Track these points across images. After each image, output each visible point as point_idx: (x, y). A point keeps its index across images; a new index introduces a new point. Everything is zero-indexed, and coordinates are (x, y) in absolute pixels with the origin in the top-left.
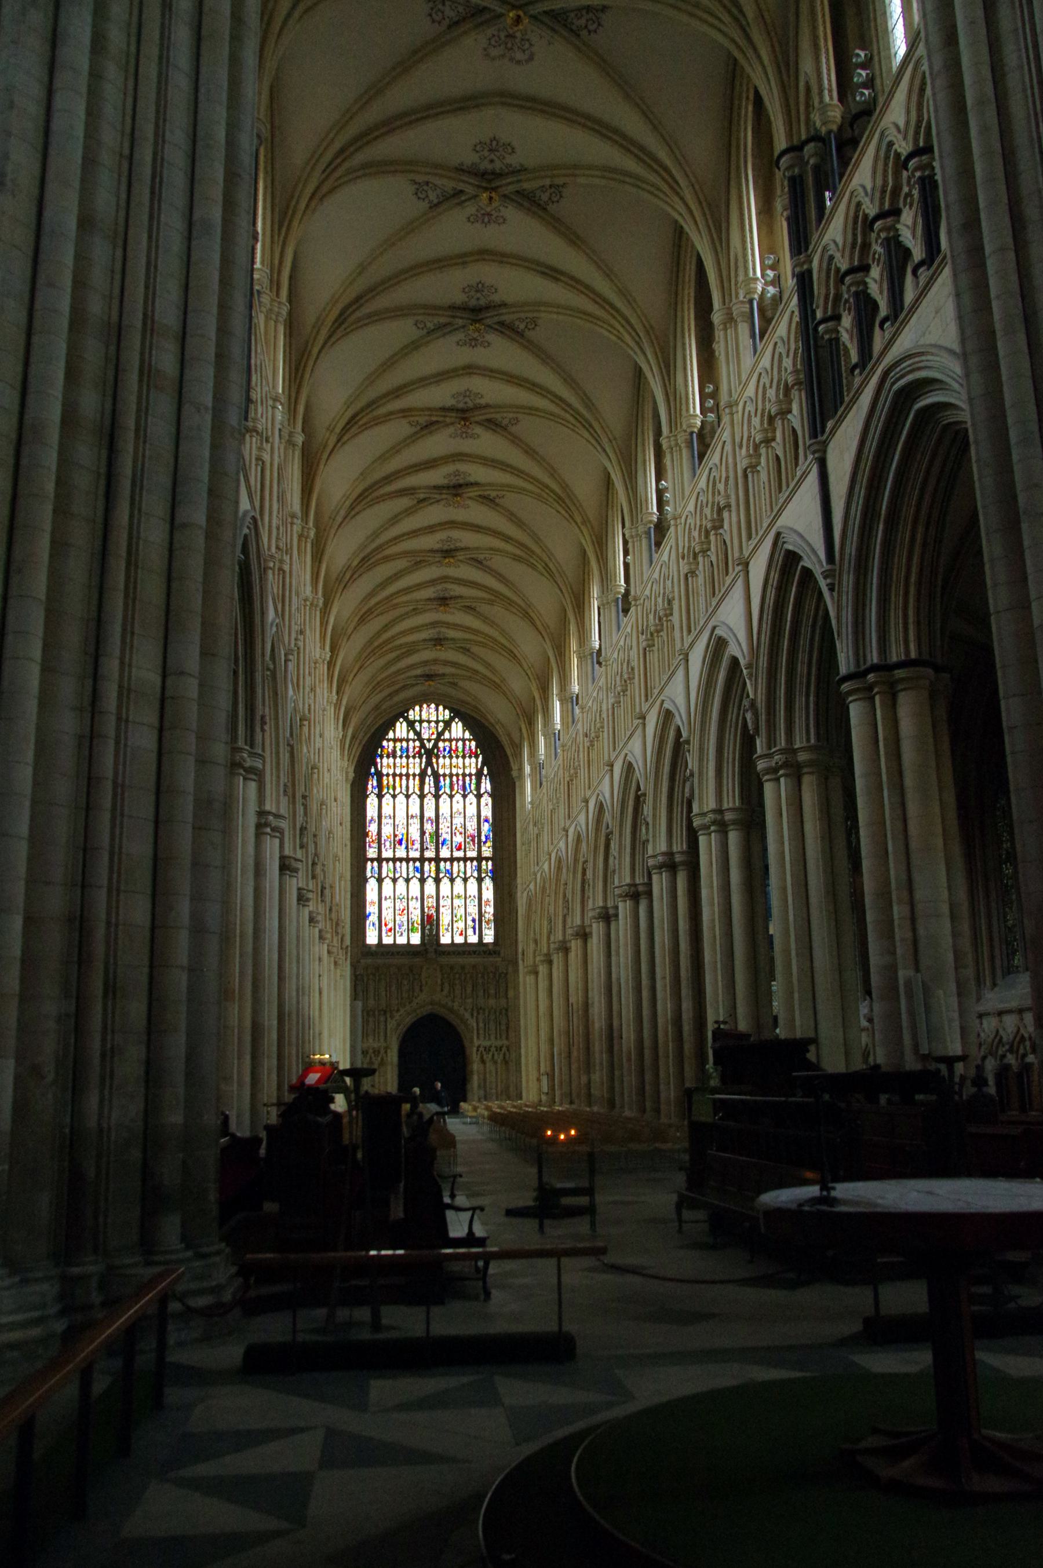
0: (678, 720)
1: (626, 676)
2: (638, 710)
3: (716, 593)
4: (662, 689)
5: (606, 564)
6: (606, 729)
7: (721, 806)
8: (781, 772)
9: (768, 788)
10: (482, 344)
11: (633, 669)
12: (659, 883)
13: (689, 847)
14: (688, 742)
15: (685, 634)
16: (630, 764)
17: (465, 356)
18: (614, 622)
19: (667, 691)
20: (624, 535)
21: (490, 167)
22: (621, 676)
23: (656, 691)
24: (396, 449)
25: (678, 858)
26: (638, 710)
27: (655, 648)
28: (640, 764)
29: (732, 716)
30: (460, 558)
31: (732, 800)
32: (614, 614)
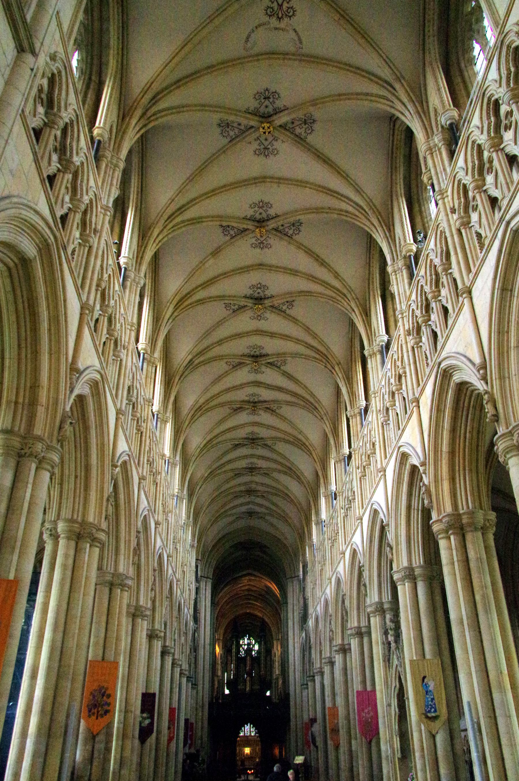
0: (381, 515)
1: (350, 498)
2: (358, 514)
3: (400, 429)
4: (371, 498)
5: (338, 440)
6: (340, 534)
7: (411, 564)
8: (450, 532)
9: (442, 544)
10: (264, 319)
11: (354, 492)
12: (375, 621)
13: (392, 598)
14: (388, 525)
15: (383, 458)
16: (355, 550)
17: (254, 325)
18: (343, 470)
19: (374, 499)
20: (347, 415)
21: (261, 217)
22: (348, 498)
23: (367, 501)
24: (219, 379)
26: (358, 514)
27: (367, 478)
28: (361, 549)
29: (415, 492)
30: (259, 443)
31: (418, 560)
32: (343, 466)
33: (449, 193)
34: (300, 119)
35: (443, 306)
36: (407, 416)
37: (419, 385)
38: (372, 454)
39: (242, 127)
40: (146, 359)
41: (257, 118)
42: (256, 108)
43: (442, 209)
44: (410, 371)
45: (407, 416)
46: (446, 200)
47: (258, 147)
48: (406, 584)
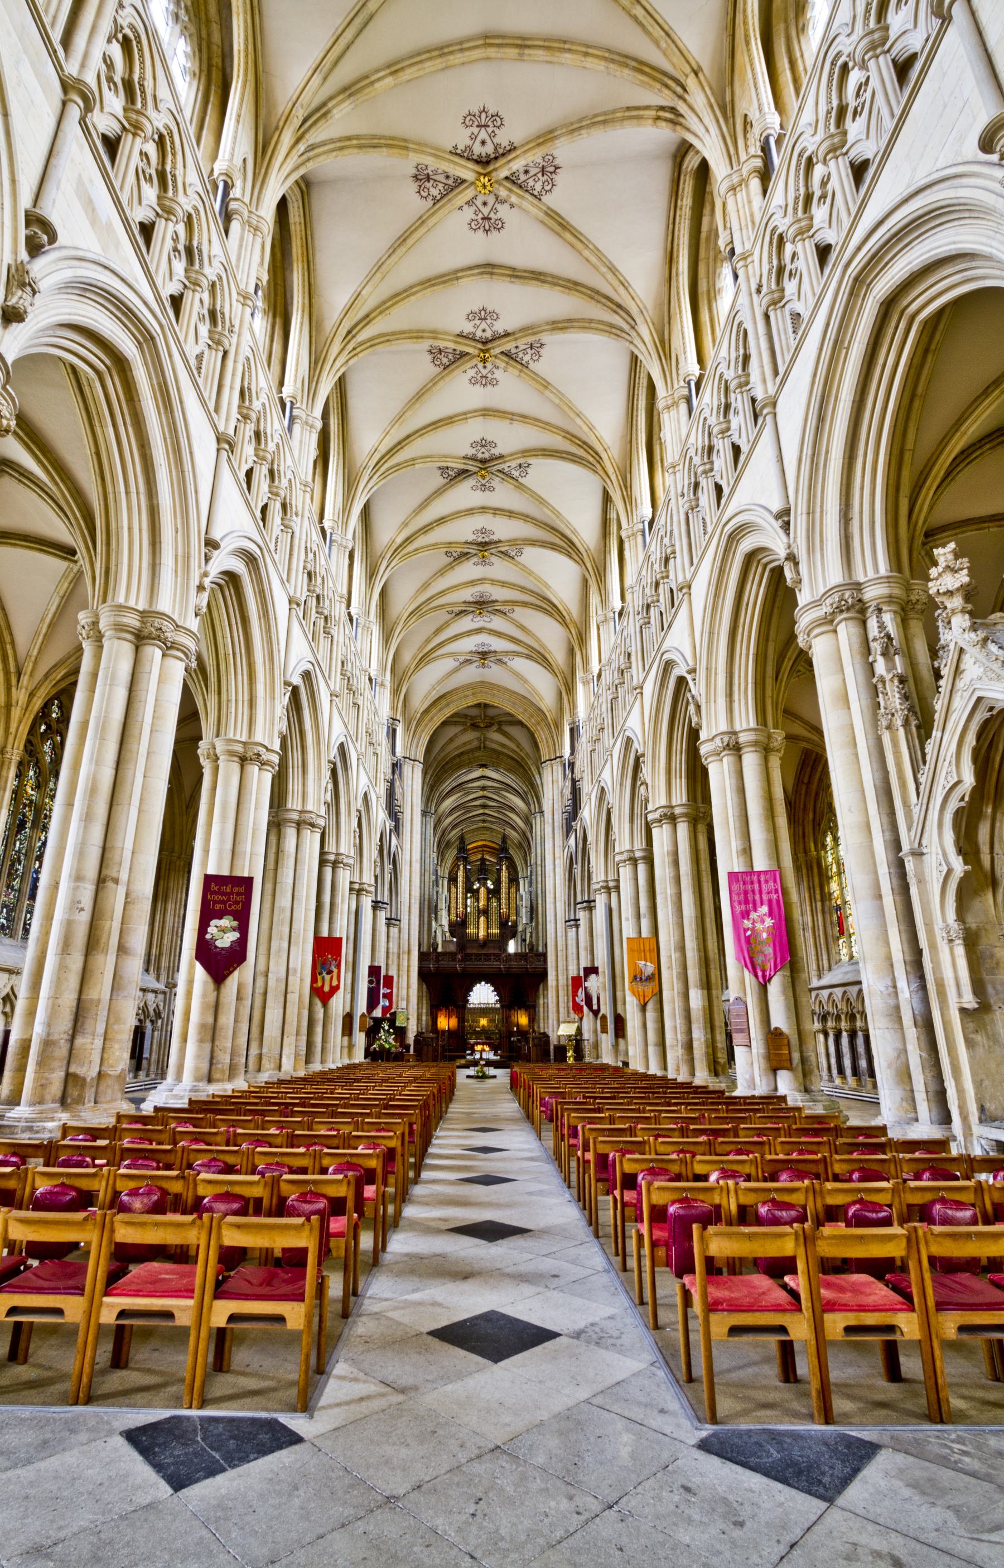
25: (678, 811)
33: (756, 257)
34: (536, 165)
35: (716, 484)
36: (707, 537)
37: (692, 564)
38: (663, 578)
39: (450, 182)
40: (297, 417)
41: (471, 165)
42: (469, 148)
43: (744, 287)
44: (681, 545)
45: (707, 537)
46: (750, 267)
47: (474, 217)
48: (725, 759)
